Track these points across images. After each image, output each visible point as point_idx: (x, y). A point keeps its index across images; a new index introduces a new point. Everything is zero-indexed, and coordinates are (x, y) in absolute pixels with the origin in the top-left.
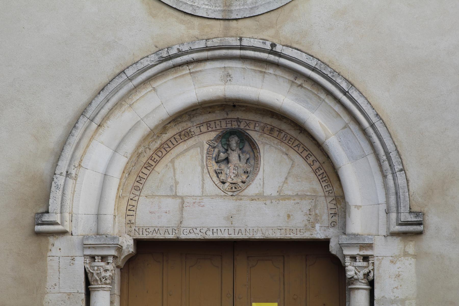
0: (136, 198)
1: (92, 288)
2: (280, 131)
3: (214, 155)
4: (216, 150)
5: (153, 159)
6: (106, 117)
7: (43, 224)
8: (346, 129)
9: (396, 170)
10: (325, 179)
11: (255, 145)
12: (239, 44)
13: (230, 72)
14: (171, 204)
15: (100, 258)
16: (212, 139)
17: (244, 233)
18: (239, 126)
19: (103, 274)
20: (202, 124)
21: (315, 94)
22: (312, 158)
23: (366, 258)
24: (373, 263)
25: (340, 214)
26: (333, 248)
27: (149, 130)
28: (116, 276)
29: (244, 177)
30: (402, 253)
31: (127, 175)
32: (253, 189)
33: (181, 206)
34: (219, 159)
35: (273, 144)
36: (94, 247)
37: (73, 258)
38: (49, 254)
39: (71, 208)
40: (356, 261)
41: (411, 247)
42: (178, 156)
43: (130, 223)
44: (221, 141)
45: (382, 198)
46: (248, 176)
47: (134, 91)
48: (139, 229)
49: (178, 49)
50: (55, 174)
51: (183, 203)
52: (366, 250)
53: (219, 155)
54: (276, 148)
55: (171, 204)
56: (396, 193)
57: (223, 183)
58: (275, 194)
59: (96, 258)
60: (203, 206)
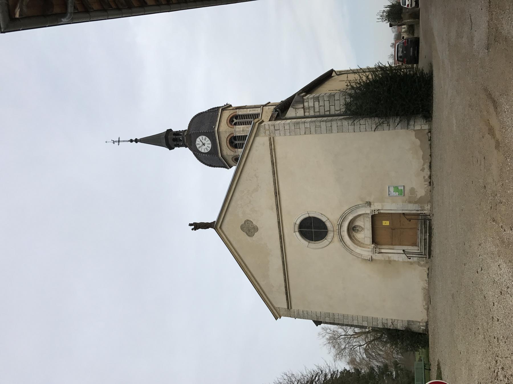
32: (363, 226)
55: (366, 239)
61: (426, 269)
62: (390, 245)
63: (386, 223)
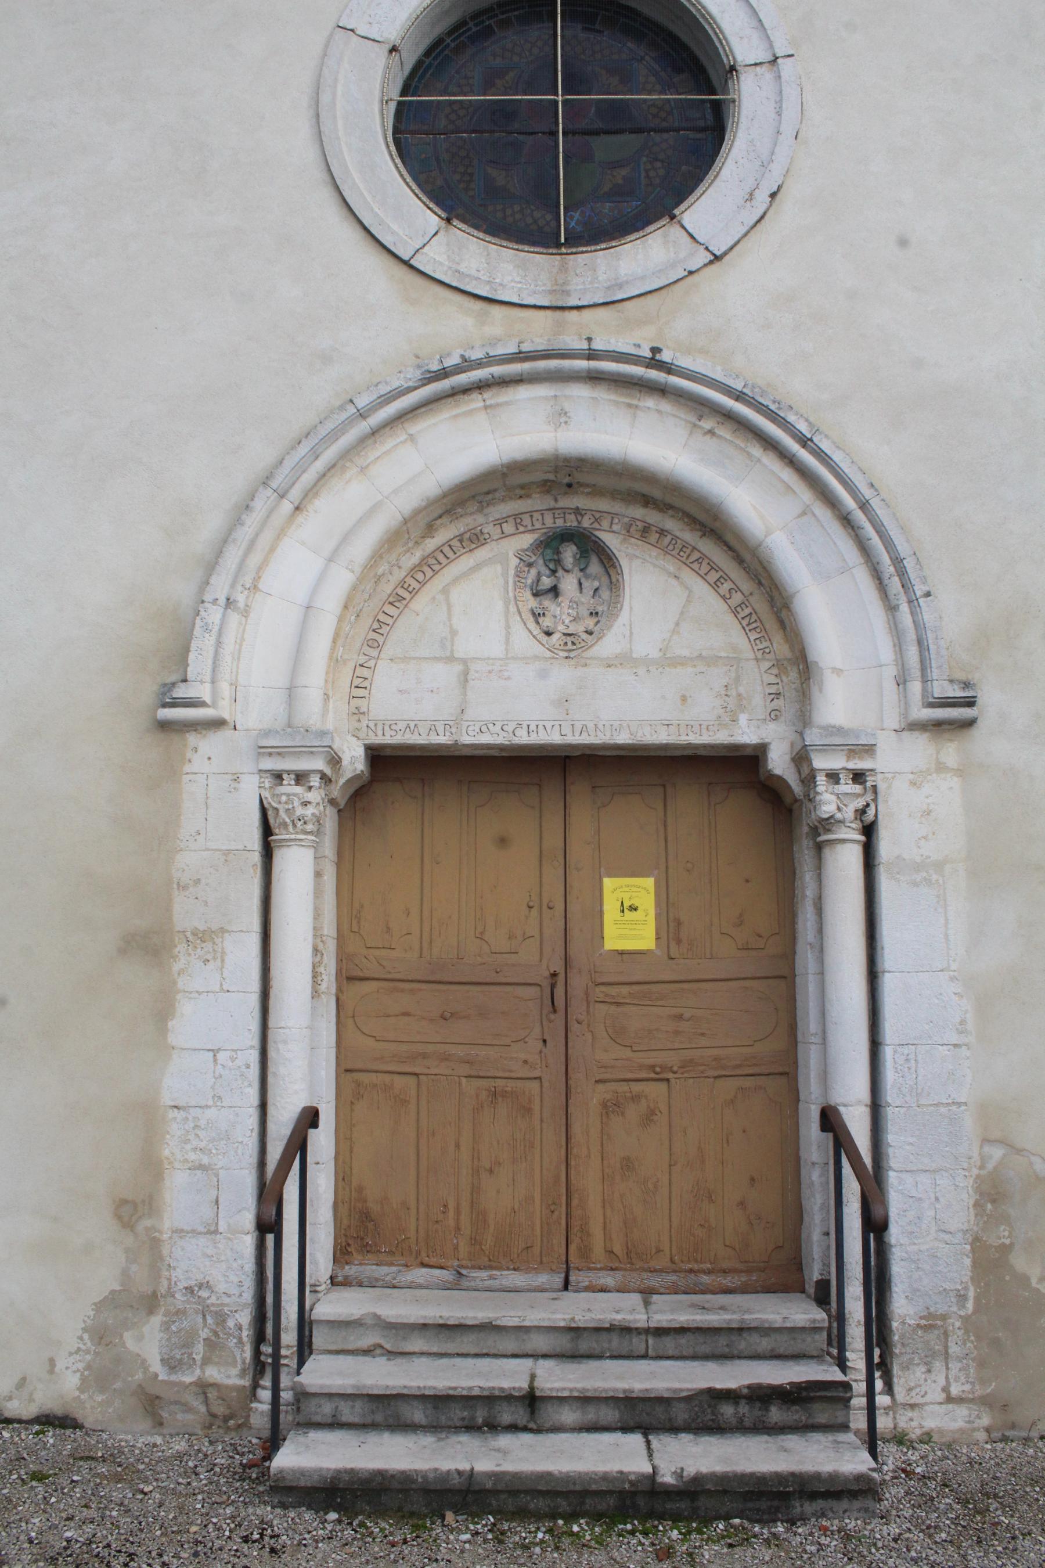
0: (371, 663)
1: (275, 841)
2: (662, 532)
3: (529, 581)
4: (533, 572)
5: (406, 586)
6: (312, 492)
7: (174, 704)
8: (805, 518)
9: (919, 593)
10: (754, 625)
11: (611, 559)
12: (586, 347)
13: (567, 406)
14: (444, 675)
15: (293, 776)
16: (525, 547)
17: (592, 733)
18: (579, 523)
19: (300, 811)
20: (505, 520)
21: (741, 449)
22: (727, 586)
23: (858, 777)
24: (874, 787)
25: (787, 694)
26: (778, 762)
27: (400, 518)
28: (327, 819)
29: (590, 623)
30: (933, 766)
31: (353, 618)
32: (609, 645)
33: (462, 678)
34: (539, 588)
35: (648, 558)
36: (278, 752)
37: (235, 777)
38: (187, 768)
39: (234, 673)
40: (837, 782)
41: (951, 751)
42: (456, 580)
43: (358, 713)
44: (542, 554)
45: (886, 653)
46: (598, 622)
47: (370, 441)
48: (376, 725)
49: (462, 356)
50: (203, 602)
51: (466, 673)
52: (861, 759)
53: (538, 581)
54: (655, 566)
55: (444, 675)
56: (920, 642)
57: (549, 634)
58: (655, 654)
59: (285, 776)
60: (509, 678)
61: (64, 1387)
62: (343, 957)
63: (629, 915)
